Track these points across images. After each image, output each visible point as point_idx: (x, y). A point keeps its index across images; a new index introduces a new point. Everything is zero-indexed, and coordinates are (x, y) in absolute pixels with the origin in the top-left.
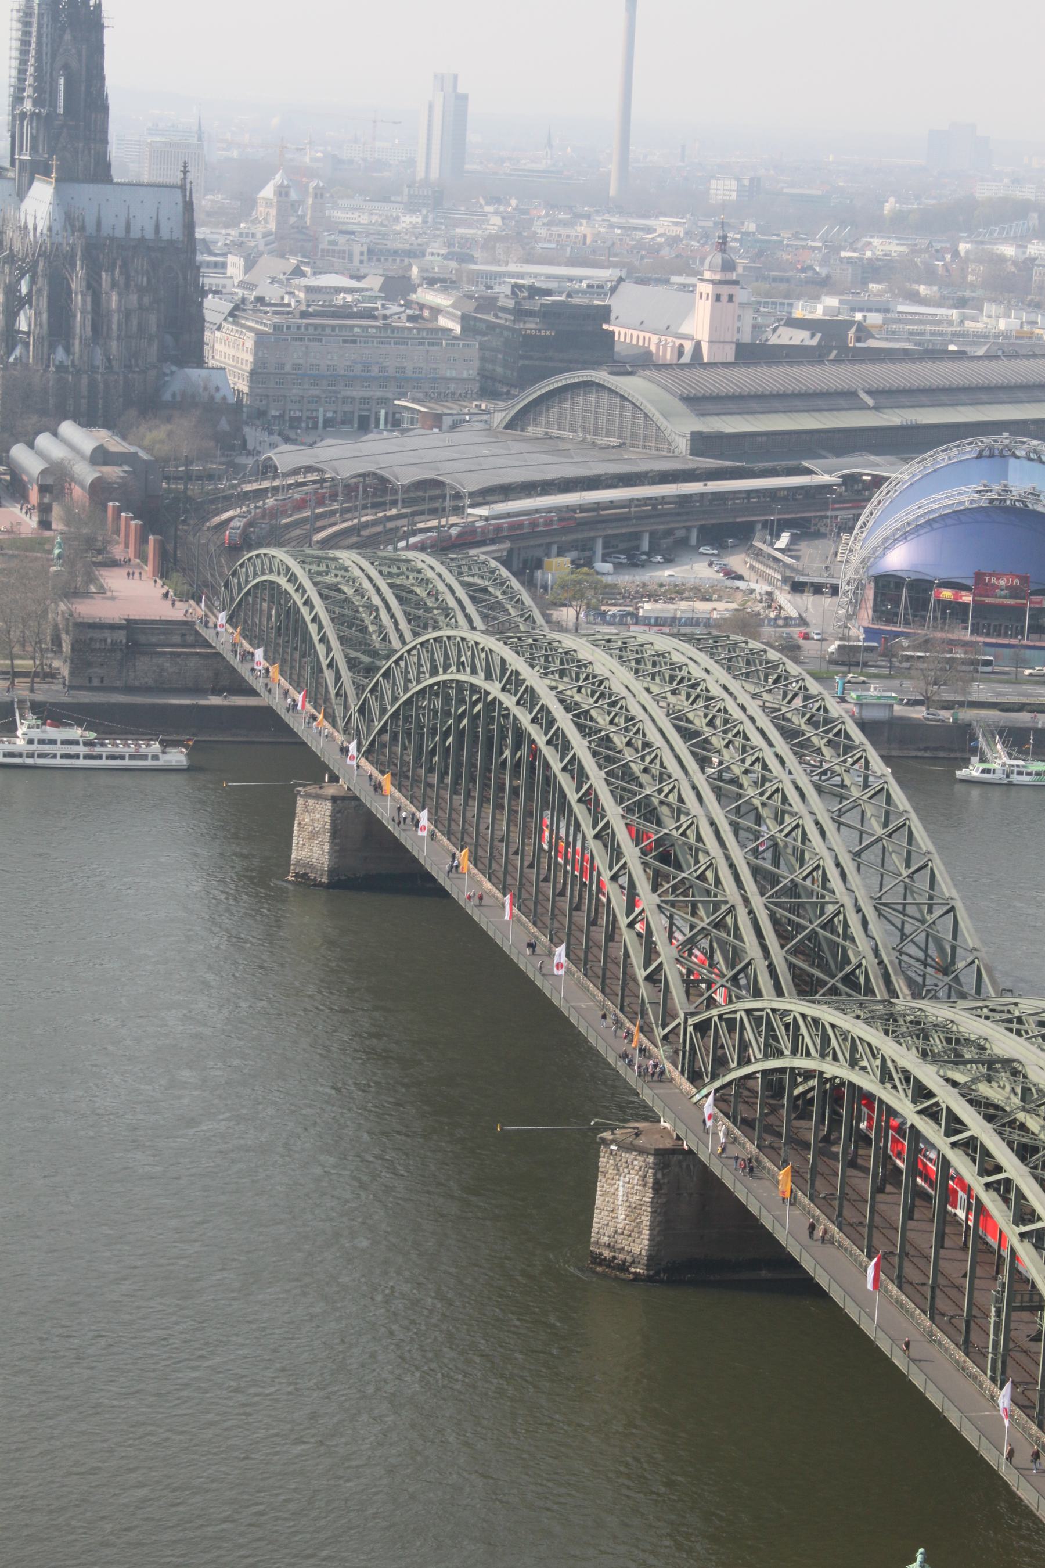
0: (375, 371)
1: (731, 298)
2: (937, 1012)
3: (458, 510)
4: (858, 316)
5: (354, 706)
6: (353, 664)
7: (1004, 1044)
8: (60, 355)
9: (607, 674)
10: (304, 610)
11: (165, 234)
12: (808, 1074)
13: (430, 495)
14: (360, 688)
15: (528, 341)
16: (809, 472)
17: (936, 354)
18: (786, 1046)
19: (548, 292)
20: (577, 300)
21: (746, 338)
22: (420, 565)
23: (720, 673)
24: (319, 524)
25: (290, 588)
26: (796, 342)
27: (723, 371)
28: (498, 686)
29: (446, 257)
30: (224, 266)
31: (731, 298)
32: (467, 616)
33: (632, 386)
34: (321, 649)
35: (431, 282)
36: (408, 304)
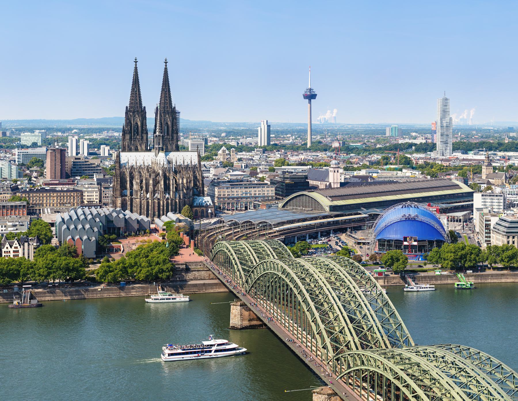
0: (248, 195)
1: (338, 171)
2: (397, 351)
3: (271, 229)
4: (371, 174)
5: (244, 280)
6: (244, 270)
7: (415, 359)
8: (167, 196)
9: (309, 268)
10: (231, 257)
11: (193, 164)
12: (366, 370)
13: (265, 226)
14: (246, 275)
15: (287, 185)
16: (360, 214)
17: (391, 182)
18: (359, 362)
19: (292, 172)
20: (299, 174)
21: (343, 181)
22: (260, 243)
23: (338, 266)
24: (235, 234)
25: (227, 251)
26: (355, 181)
27: (337, 190)
28: (281, 273)
29: (266, 165)
30: (209, 171)
31: (338, 171)
32: (273, 256)
33: (314, 195)
34: (235, 266)
35: (262, 172)
36: (256, 177)
